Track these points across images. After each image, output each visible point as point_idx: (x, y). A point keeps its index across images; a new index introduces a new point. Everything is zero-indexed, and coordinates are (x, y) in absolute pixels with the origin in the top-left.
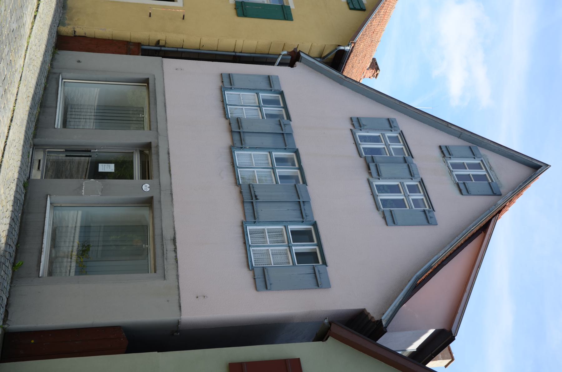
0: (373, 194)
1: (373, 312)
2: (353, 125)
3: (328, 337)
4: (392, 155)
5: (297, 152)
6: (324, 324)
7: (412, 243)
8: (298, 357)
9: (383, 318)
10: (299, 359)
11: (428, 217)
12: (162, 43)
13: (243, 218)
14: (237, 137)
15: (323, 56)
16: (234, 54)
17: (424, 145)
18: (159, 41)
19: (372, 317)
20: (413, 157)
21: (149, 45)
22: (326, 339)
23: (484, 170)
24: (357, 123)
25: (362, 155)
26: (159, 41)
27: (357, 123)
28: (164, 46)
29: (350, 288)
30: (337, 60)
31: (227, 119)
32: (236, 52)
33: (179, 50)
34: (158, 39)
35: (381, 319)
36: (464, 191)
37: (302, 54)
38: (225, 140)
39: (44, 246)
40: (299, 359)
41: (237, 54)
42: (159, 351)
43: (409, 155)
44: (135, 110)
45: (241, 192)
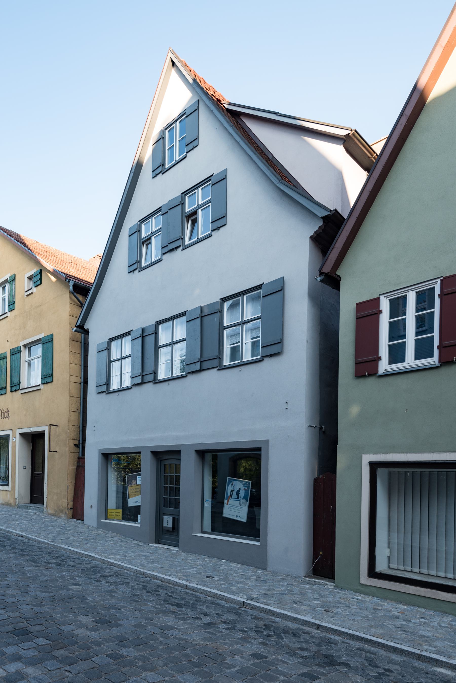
0: (200, 241)
1: (313, 227)
2: (135, 270)
3: (336, 275)
4: (210, 200)
5: (224, 300)
6: (322, 281)
7: (246, 191)
8: (355, 306)
9: (320, 215)
10: (357, 304)
11: (218, 181)
12: (76, 443)
13: (216, 369)
14: (206, 365)
15: (80, 305)
16: (82, 383)
17: (155, 193)
18: (75, 445)
19: (320, 227)
20: (213, 175)
21: (79, 453)
22: (339, 276)
23: (175, 125)
24: (135, 266)
25: (209, 234)
26: (75, 445)
27: (135, 266)
28: (79, 440)
29: (289, 255)
30: (83, 292)
31: (187, 376)
32: (81, 382)
33: (81, 429)
34: (73, 445)
35: (322, 218)
36: (194, 144)
37: (78, 324)
38: (211, 376)
39: (236, 541)
40: (357, 304)
41: (82, 381)
42: (336, 444)
43: (210, 180)
44: (123, 463)
45: (271, 356)
